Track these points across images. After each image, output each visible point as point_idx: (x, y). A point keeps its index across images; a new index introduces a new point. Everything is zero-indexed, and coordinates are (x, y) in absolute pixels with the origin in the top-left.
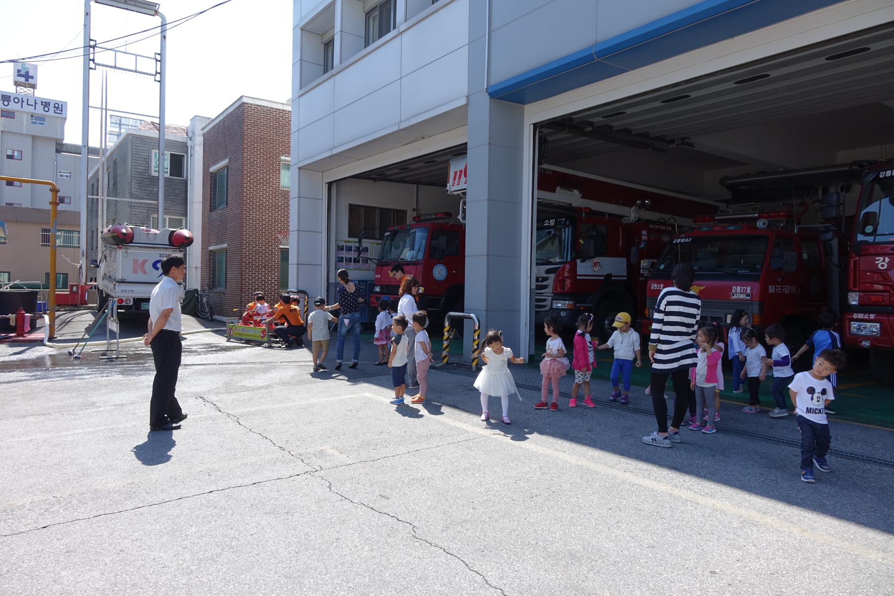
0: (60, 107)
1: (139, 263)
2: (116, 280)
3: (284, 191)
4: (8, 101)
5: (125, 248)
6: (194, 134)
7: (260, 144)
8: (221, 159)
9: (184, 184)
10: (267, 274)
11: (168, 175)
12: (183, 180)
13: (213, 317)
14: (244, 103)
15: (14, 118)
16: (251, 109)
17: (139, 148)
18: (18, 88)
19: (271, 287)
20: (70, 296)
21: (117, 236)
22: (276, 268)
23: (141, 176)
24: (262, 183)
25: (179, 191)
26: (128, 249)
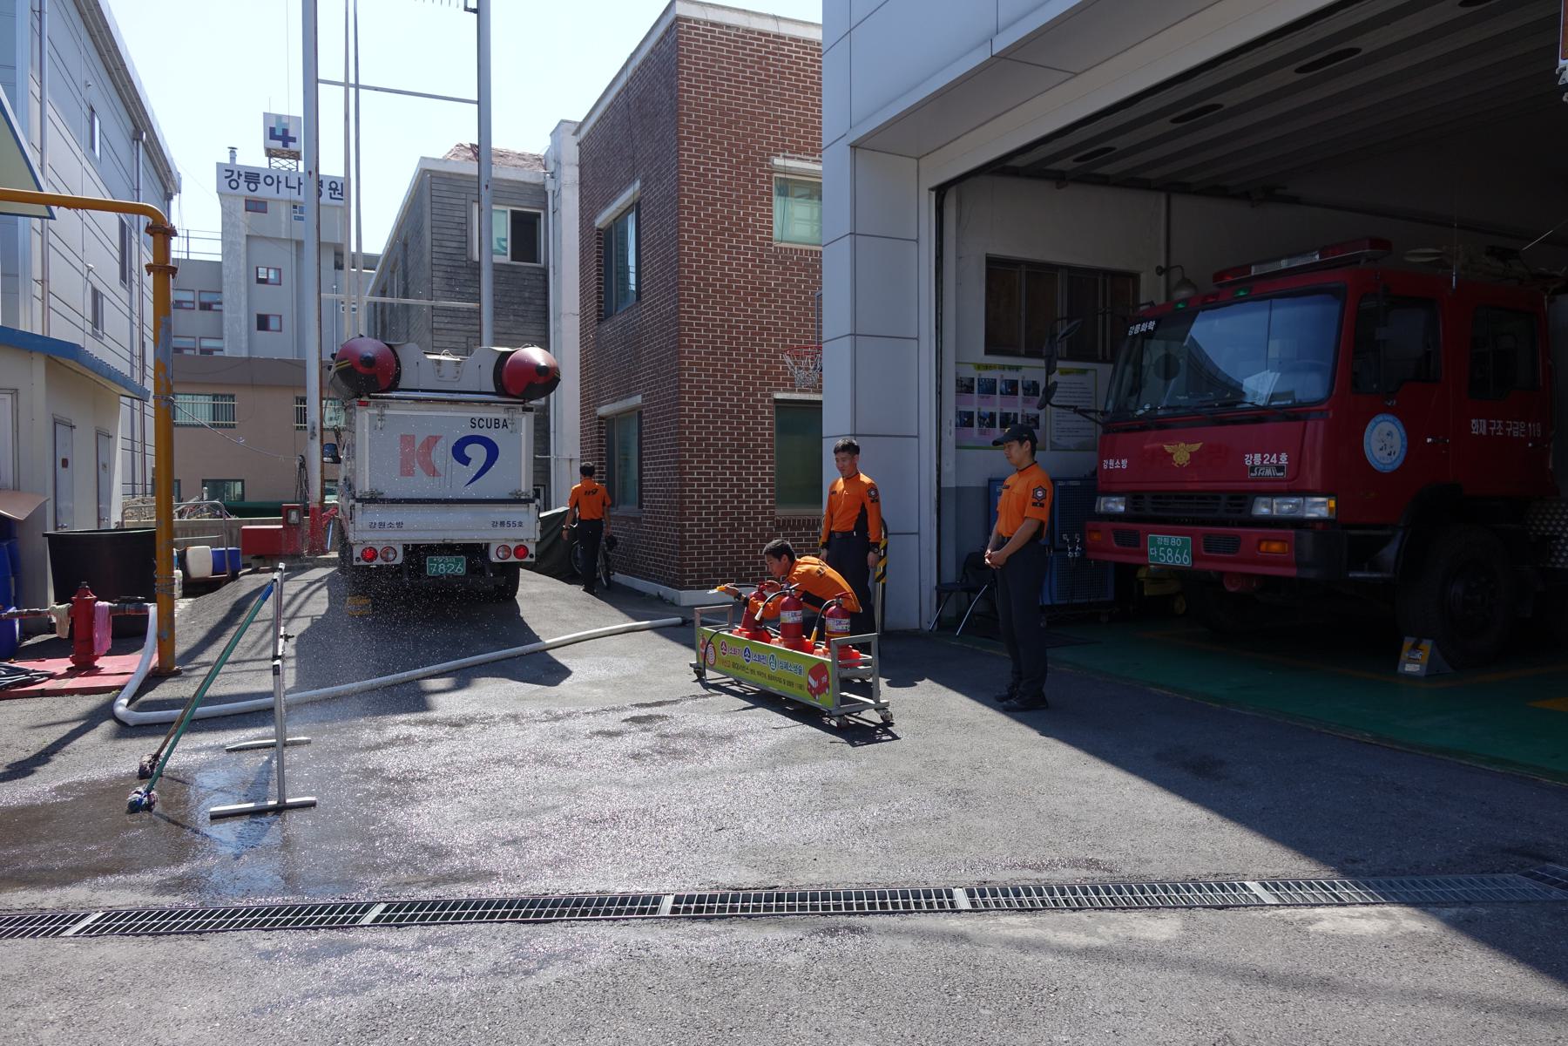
0: (339, 187)
1: (417, 446)
2: (357, 496)
3: (781, 248)
4: (255, 183)
5: (377, 405)
6: (558, 162)
7: (720, 125)
8: (622, 190)
9: (541, 278)
10: (744, 468)
11: (507, 259)
12: (538, 268)
13: (612, 577)
14: (678, 18)
15: (266, 212)
16: (696, 34)
17: (446, 200)
18: (272, 161)
19: (754, 502)
20: (284, 535)
21: (352, 367)
22: (768, 452)
23: (451, 263)
24: (727, 229)
25: (530, 292)
26: (385, 406)
